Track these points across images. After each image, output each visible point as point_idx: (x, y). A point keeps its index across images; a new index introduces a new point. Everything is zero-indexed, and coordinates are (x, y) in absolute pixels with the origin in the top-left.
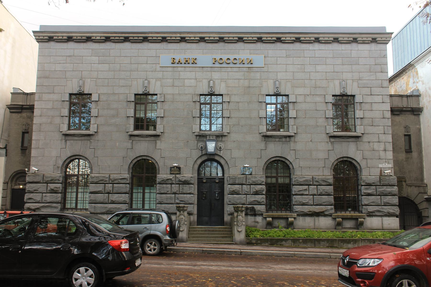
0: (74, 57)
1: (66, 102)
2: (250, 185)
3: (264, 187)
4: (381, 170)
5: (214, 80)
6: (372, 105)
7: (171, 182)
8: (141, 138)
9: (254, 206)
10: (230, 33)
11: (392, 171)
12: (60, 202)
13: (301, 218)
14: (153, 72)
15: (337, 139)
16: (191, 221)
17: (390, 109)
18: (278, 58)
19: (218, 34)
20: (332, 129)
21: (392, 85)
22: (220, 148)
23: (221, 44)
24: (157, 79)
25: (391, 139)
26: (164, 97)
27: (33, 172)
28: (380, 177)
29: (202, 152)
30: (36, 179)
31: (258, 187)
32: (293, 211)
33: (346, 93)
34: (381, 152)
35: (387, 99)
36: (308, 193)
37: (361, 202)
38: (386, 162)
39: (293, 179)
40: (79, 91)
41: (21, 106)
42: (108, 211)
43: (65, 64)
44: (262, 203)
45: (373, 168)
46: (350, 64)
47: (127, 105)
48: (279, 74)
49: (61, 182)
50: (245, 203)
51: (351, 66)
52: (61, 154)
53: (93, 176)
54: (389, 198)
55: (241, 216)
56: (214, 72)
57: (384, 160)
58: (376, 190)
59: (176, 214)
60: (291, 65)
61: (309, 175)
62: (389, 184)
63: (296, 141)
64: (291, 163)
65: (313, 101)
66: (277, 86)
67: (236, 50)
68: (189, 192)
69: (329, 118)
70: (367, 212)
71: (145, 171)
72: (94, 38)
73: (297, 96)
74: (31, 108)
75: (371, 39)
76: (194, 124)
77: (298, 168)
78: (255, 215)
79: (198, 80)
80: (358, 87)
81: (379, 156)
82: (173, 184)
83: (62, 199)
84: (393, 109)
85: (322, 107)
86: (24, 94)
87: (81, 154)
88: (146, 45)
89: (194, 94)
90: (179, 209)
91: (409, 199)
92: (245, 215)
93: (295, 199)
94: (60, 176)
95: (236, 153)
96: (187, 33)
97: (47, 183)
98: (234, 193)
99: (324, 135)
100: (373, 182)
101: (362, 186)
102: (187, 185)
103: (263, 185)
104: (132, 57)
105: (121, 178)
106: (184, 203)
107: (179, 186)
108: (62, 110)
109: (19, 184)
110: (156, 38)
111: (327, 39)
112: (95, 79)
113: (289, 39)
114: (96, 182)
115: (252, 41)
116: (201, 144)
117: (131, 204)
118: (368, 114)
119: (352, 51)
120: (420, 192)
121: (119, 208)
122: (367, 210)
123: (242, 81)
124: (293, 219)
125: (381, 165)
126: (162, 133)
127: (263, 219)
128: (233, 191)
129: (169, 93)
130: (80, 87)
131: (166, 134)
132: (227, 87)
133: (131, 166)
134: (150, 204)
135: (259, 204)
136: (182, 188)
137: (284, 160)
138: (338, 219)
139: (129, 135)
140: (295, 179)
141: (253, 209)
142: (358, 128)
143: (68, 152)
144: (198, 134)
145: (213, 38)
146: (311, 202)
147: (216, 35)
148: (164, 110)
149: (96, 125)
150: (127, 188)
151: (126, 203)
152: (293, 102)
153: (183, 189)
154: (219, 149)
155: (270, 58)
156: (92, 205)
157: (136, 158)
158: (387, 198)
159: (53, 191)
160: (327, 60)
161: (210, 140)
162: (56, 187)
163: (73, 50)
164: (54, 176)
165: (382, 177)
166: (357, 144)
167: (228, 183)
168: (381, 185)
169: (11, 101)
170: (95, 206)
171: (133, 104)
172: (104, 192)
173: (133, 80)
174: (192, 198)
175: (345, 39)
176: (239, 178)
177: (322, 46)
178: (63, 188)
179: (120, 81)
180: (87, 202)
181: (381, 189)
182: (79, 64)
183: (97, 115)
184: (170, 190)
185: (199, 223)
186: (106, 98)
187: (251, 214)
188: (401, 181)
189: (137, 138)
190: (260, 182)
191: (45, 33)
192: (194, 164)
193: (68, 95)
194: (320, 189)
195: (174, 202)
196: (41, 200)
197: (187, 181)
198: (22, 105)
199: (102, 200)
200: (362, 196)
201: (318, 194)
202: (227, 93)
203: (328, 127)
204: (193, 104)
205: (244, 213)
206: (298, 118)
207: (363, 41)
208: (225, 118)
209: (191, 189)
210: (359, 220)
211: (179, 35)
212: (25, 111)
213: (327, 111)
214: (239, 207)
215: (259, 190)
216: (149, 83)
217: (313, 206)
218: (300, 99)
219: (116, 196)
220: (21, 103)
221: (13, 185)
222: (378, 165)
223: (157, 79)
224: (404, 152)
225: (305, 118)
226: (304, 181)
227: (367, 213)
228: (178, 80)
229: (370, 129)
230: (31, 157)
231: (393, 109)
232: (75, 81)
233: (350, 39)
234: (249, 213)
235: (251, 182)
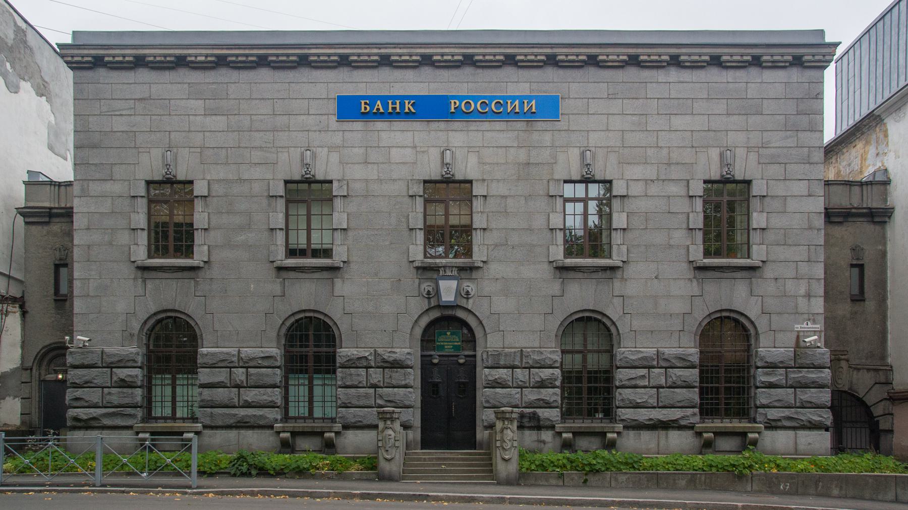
0: (152, 101)
1: (139, 199)
2: (529, 368)
3: (557, 372)
4: (798, 337)
5: (454, 149)
7: (365, 364)
8: (300, 274)
9: (538, 410)
10: (486, 45)
11: (820, 337)
12: (139, 405)
13: (632, 433)
14: (322, 132)
15: (710, 274)
16: (408, 440)
17: (823, 210)
18: (590, 101)
19: (462, 48)
20: (697, 253)
21: (831, 161)
22: (468, 293)
23: (468, 70)
24: (332, 148)
25: (822, 271)
26: (348, 186)
27: (81, 345)
28: (795, 351)
29: (429, 303)
31: (545, 373)
32: (616, 420)
33: (733, 176)
34: (800, 299)
35: (820, 190)
36: (647, 384)
37: (755, 401)
38: (809, 320)
39: (618, 355)
40: (167, 174)
41: (48, 210)
42: (239, 422)
43: (132, 117)
44: (552, 405)
46: (743, 112)
47: (269, 205)
48: (591, 135)
49: (139, 364)
50: (518, 405)
51: (745, 117)
52: (136, 309)
53: (206, 352)
55: (509, 430)
56: (454, 132)
57: (806, 316)
58: (787, 376)
59: (376, 427)
60: (618, 116)
62: (813, 364)
63: (625, 277)
64: (614, 323)
65: (663, 194)
66: (588, 162)
67: (499, 84)
68: (403, 383)
69: (695, 229)
70: (766, 420)
71: (311, 343)
72: (193, 59)
73: (630, 183)
74: (68, 214)
75: (790, 58)
76: (413, 244)
77: (628, 332)
78: (539, 428)
79: (418, 149)
80: (759, 163)
82: (371, 367)
83: (143, 398)
84: (831, 210)
85: (682, 206)
86: (52, 183)
87: (177, 308)
88: (305, 74)
89: (411, 180)
90: (384, 417)
91: (853, 396)
92: (518, 427)
93: (622, 395)
95: (501, 304)
96: (394, 46)
97: (111, 366)
98: (497, 385)
99: (685, 265)
100: (781, 360)
101: (758, 368)
102: (399, 370)
103: (557, 368)
104: (275, 100)
105: (262, 355)
106: (393, 404)
107: (384, 371)
108: (132, 215)
109: (54, 370)
110: (326, 58)
111: (697, 58)
112: (199, 150)
114: (212, 364)
115: (535, 64)
116: (427, 286)
117: (285, 408)
118: (777, 221)
119: (749, 85)
120: (877, 382)
121: (260, 415)
122: (766, 417)
123: (512, 150)
124: (615, 435)
125: (799, 326)
126: (344, 262)
127: (554, 437)
128: (495, 381)
130: (168, 167)
131: (352, 265)
132: (481, 163)
133: (284, 331)
134: (324, 407)
135: (549, 405)
136: (388, 376)
137: (599, 317)
138: (705, 435)
139: (276, 268)
140: (622, 357)
141: (534, 417)
142: (754, 248)
143: (151, 303)
144: (420, 265)
145: (449, 58)
146: (653, 401)
147: (457, 51)
148: (348, 215)
149: (206, 248)
150: (277, 376)
151: (275, 405)
152: (620, 196)
153: (390, 377)
154: (465, 296)
155: (573, 100)
156: (205, 411)
157: (293, 314)
158: (808, 392)
160: (695, 104)
162: (130, 376)
163: (148, 85)
165: (799, 351)
166: (751, 283)
167: (484, 365)
168: (797, 366)
169: (26, 200)
170: (212, 413)
171: (281, 204)
172: (229, 385)
173: (279, 150)
174: (410, 396)
175: (735, 58)
176: (506, 355)
177: (686, 75)
178: (144, 376)
179: (252, 153)
180: (196, 404)
181: (794, 375)
182: (163, 118)
183: (206, 227)
184: (365, 380)
185: (426, 443)
186: (225, 190)
187: (530, 425)
188: (836, 359)
189: (292, 274)
191: (84, 49)
192: (413, 328)
193: (143, 183)
194: (673, 376)
195: (373, 403)
196: (100, 401)
197: (400, 362)
198: (51, 208)
199: (226, 401)
200: (757, 388)
201: (668, 385)
202: (481, 178)
203: (692, 247)
204: (407, 200)
205: (515, 424)
206: (631, 229)
207: (773, 62)
208: (478, 231)
209: (407, 376)
210: (750, 435)
211: (375, 51)
212: (57, 220)
213: (691, 215)
214: (506, 413)
215: (548, 379)
217: (657, 409)
218: (636, 189)
219: (254, 393)
220: (47, 204)
221: (43, 372)
222: (794, 326)
223: (332, 148)
224: (849, 300)
225: (646, 228)
226: (639, 359)
227: (766, 423)
228: (377, 149)
229: (782, 253)
231: (831, 210)
232: (156, 153)
233: (745, 58)
235: (531, 362)
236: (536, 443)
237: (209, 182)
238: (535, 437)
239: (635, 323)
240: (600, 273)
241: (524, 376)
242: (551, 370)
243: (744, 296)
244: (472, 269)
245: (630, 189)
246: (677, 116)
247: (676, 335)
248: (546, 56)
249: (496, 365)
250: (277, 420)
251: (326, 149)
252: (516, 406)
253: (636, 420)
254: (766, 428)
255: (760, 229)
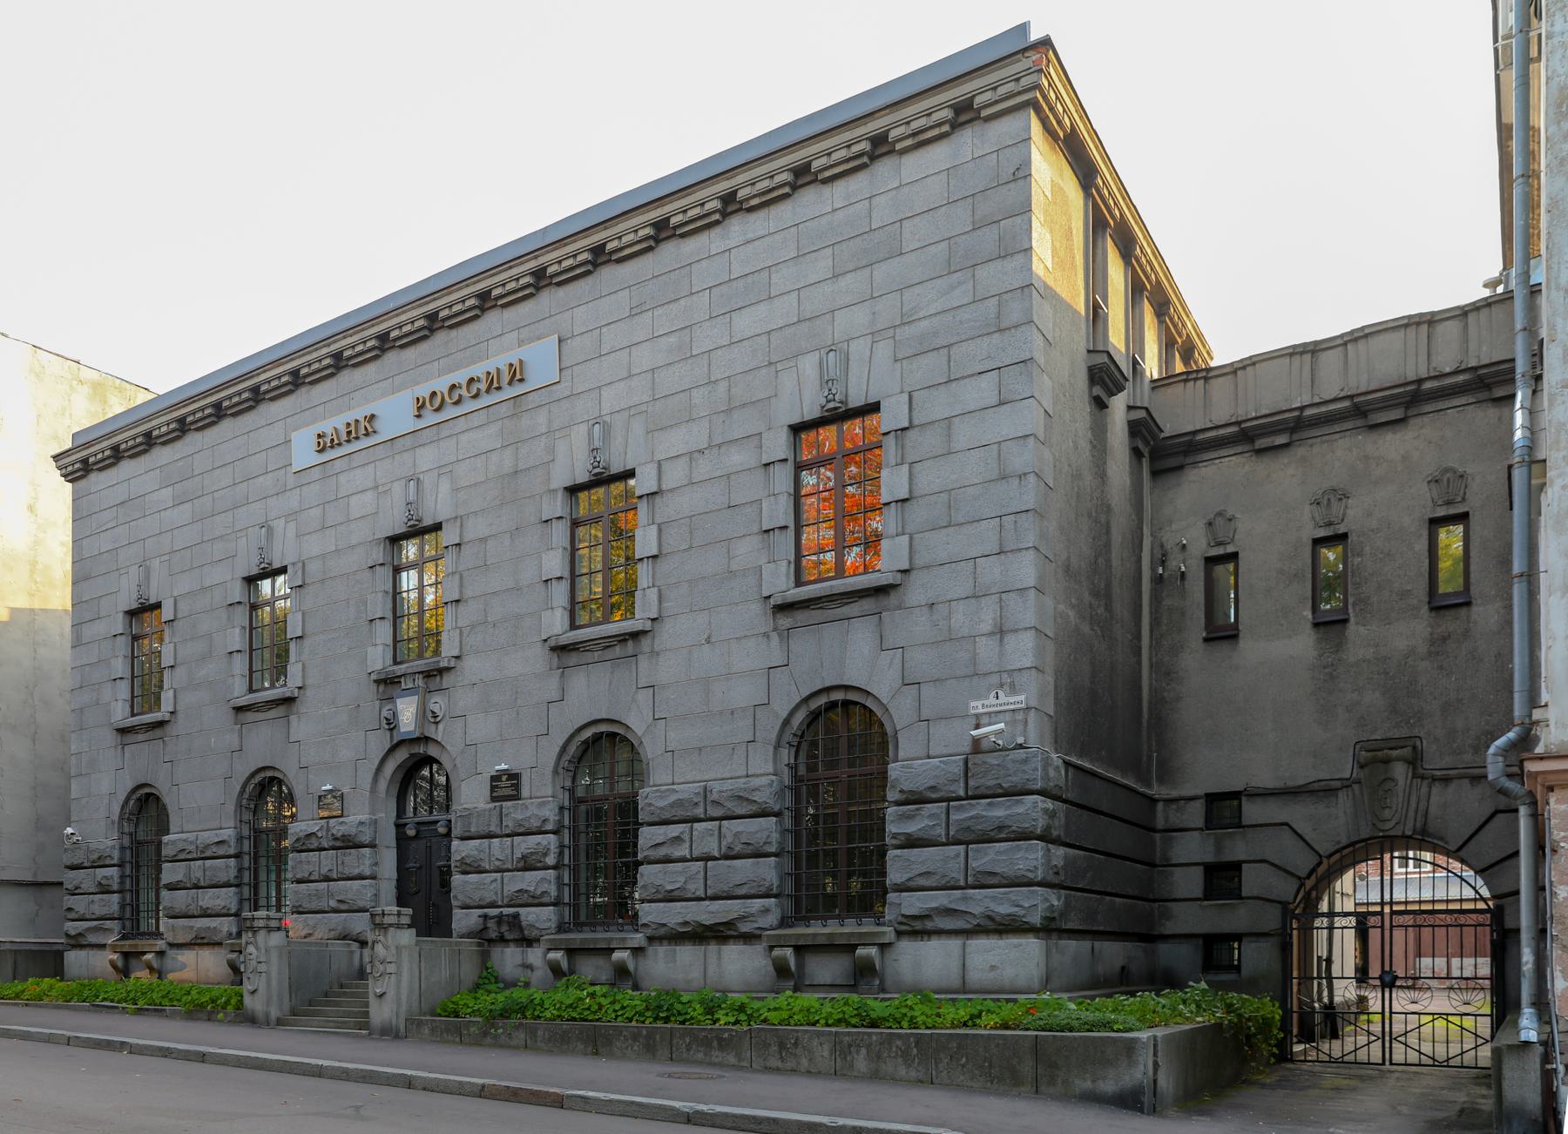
6: (949, 428)
9: (522, 911)
12: (116, 916)
13: (662, 950)
15: (802, 616)
38: (1001, 686)
45: (943, 722)
46: (864, 263)
51: (867, 271)
54: (999, 853)
60: (647, 343)
61: (698, 778)
62: (1000, 786)
63: (656, 649)
68: (356, 872)
78: (528, 942)
81: (974, 660)
94: (113, 847)
96: (342, 335)
99: (756, 607)
100: (932, 783)
102: (352, 850)
113: (631, 237)
118: (931, 477)
126: (300, 688)
129: (314, 554)
152: (648, 495)
159: (105, 890)
161: (408, 692)
175: (836, 156)
177: (756, 224)
190: (535, 824)
203: (767, 570)
207: (914, 135)
215: (532, 854)
216: (272, 535)
223: (291, 516)
226: (672, 805)
229: (939, 545)
233: (856, 149)
234: (508, 936)
236: (521, 969)
237: (175, 600)
238: (519, 960)
239: (672, 735)
240: (617, 648)
241: (503, 850)
242: (538, 838)
243: (867, 652)
244: (441, 671)
245: (664, 478)
246: (743, 311)
247: (741, 751)
248: (532, 274)
250: (231, 934)
251: (283, 520)
252: (493, 905)
253: (664, 925)
254: (899, 934)
255: (897, 502)
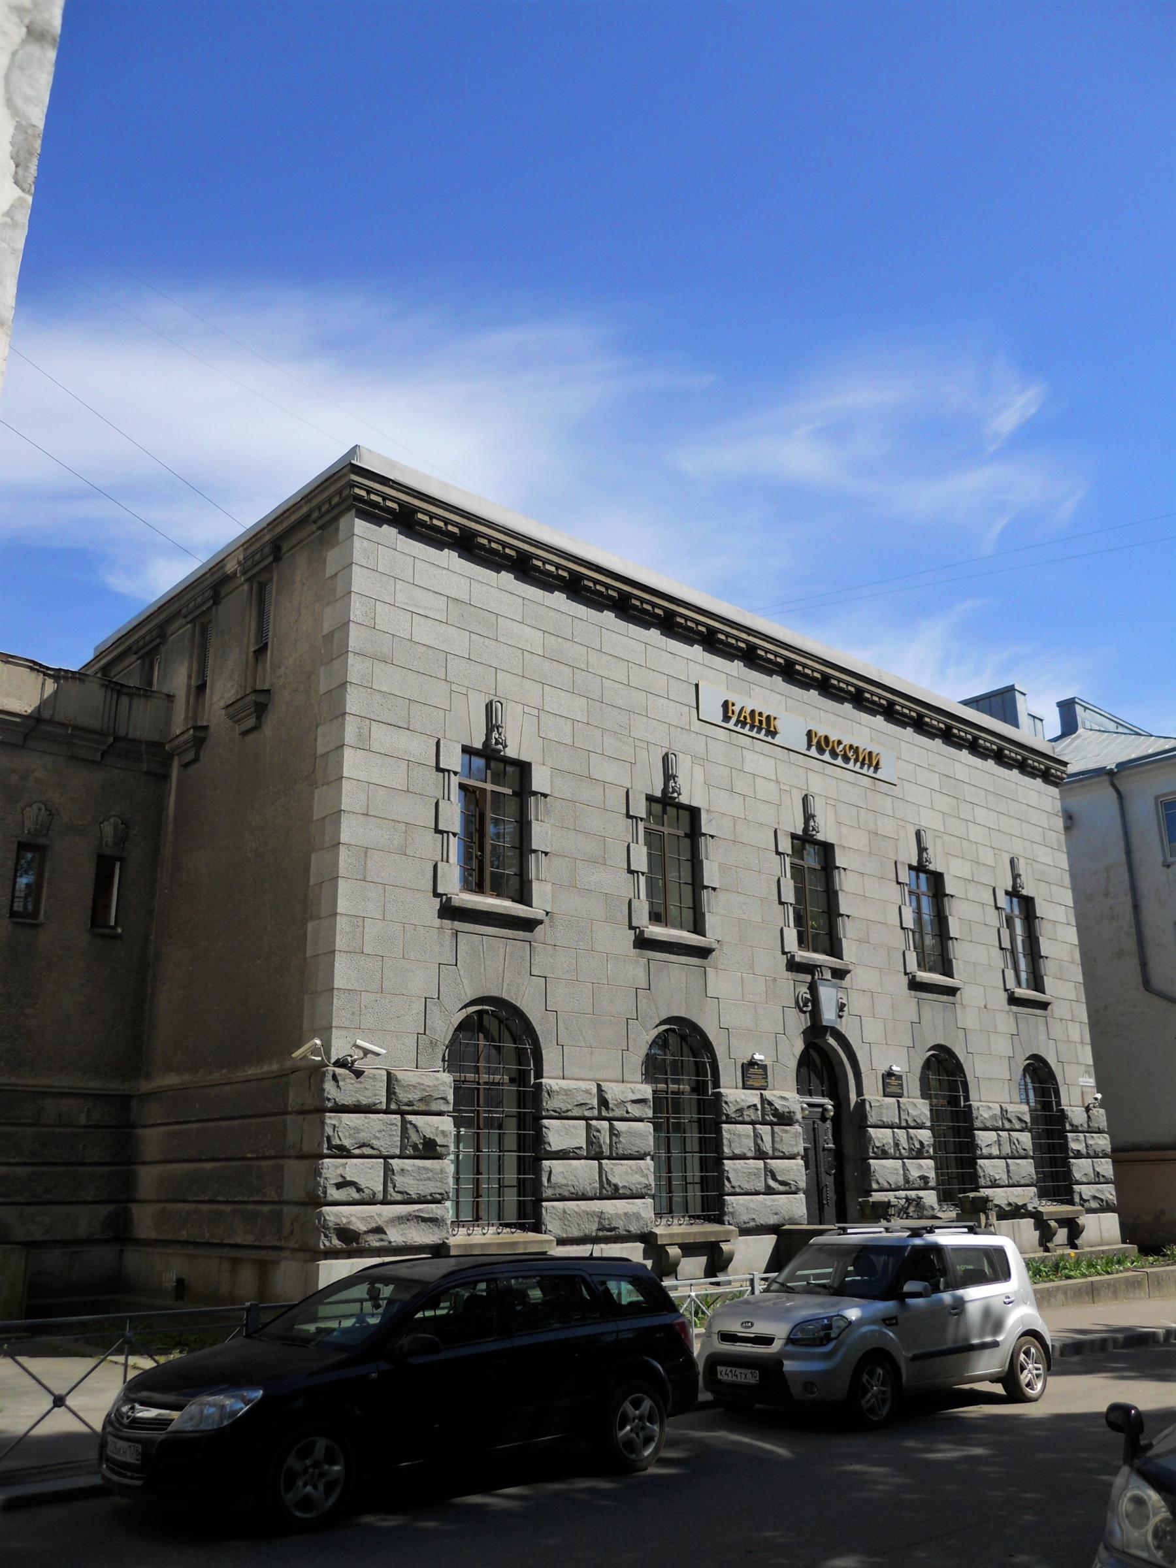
30: (368, 1093)
143: (465, 981)
164: (430, 1083)
173: (638, 743)
230: (335, 992)
249: (880, 1123)
